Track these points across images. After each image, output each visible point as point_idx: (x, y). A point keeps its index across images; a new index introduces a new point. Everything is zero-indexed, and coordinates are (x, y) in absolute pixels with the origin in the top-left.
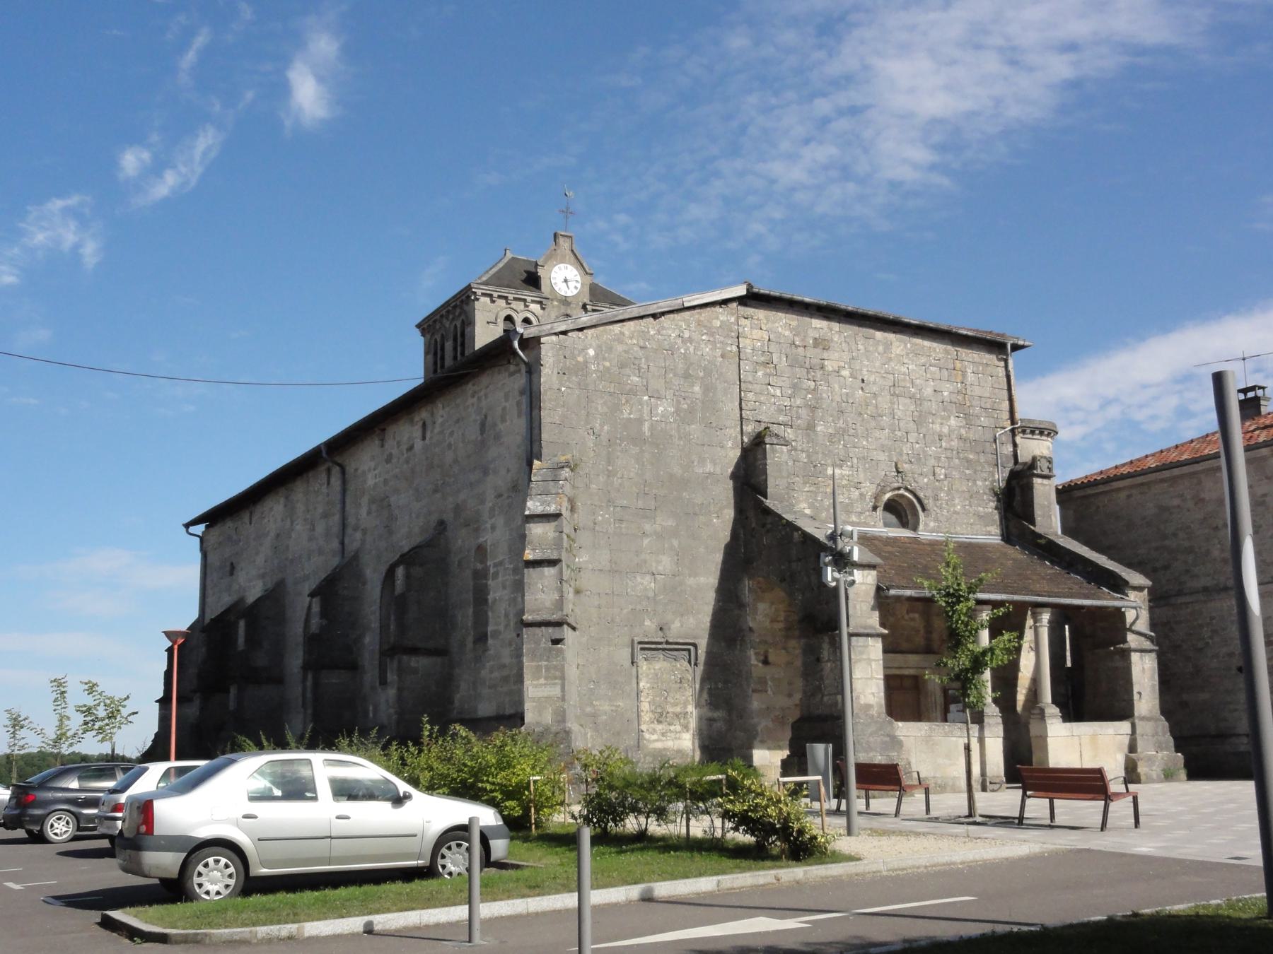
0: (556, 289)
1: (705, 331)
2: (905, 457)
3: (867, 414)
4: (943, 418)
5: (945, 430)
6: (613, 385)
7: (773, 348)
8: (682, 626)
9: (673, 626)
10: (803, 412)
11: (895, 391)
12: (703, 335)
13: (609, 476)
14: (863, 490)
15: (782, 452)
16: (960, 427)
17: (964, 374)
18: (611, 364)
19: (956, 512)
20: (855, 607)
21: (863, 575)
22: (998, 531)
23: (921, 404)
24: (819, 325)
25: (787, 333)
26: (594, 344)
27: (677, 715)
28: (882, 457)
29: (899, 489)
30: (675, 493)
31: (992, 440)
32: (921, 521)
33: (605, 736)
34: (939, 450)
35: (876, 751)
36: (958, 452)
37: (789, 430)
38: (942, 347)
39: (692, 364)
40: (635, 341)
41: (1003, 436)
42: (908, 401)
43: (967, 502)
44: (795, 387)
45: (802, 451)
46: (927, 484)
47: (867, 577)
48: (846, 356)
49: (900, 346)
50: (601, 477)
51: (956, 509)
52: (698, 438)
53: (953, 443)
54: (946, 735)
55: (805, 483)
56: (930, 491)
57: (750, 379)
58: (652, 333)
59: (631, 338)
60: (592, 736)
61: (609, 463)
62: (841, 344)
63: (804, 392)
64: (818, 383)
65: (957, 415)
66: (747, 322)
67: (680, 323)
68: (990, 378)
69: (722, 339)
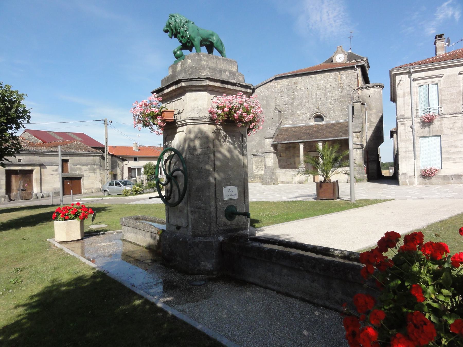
4: (333, 92)
5: (334, 95)
19: (336, 115)
24: (296, 79)
27: (261, 168)
28: (313, 106)
29: (317, 113)
34: (331, 100)
42: (321, 90)
43: (340, 112)
44: (288, 95)
54: (290, 172)
55: (290, 117)
57: (277, 96)
66: (276, 84)
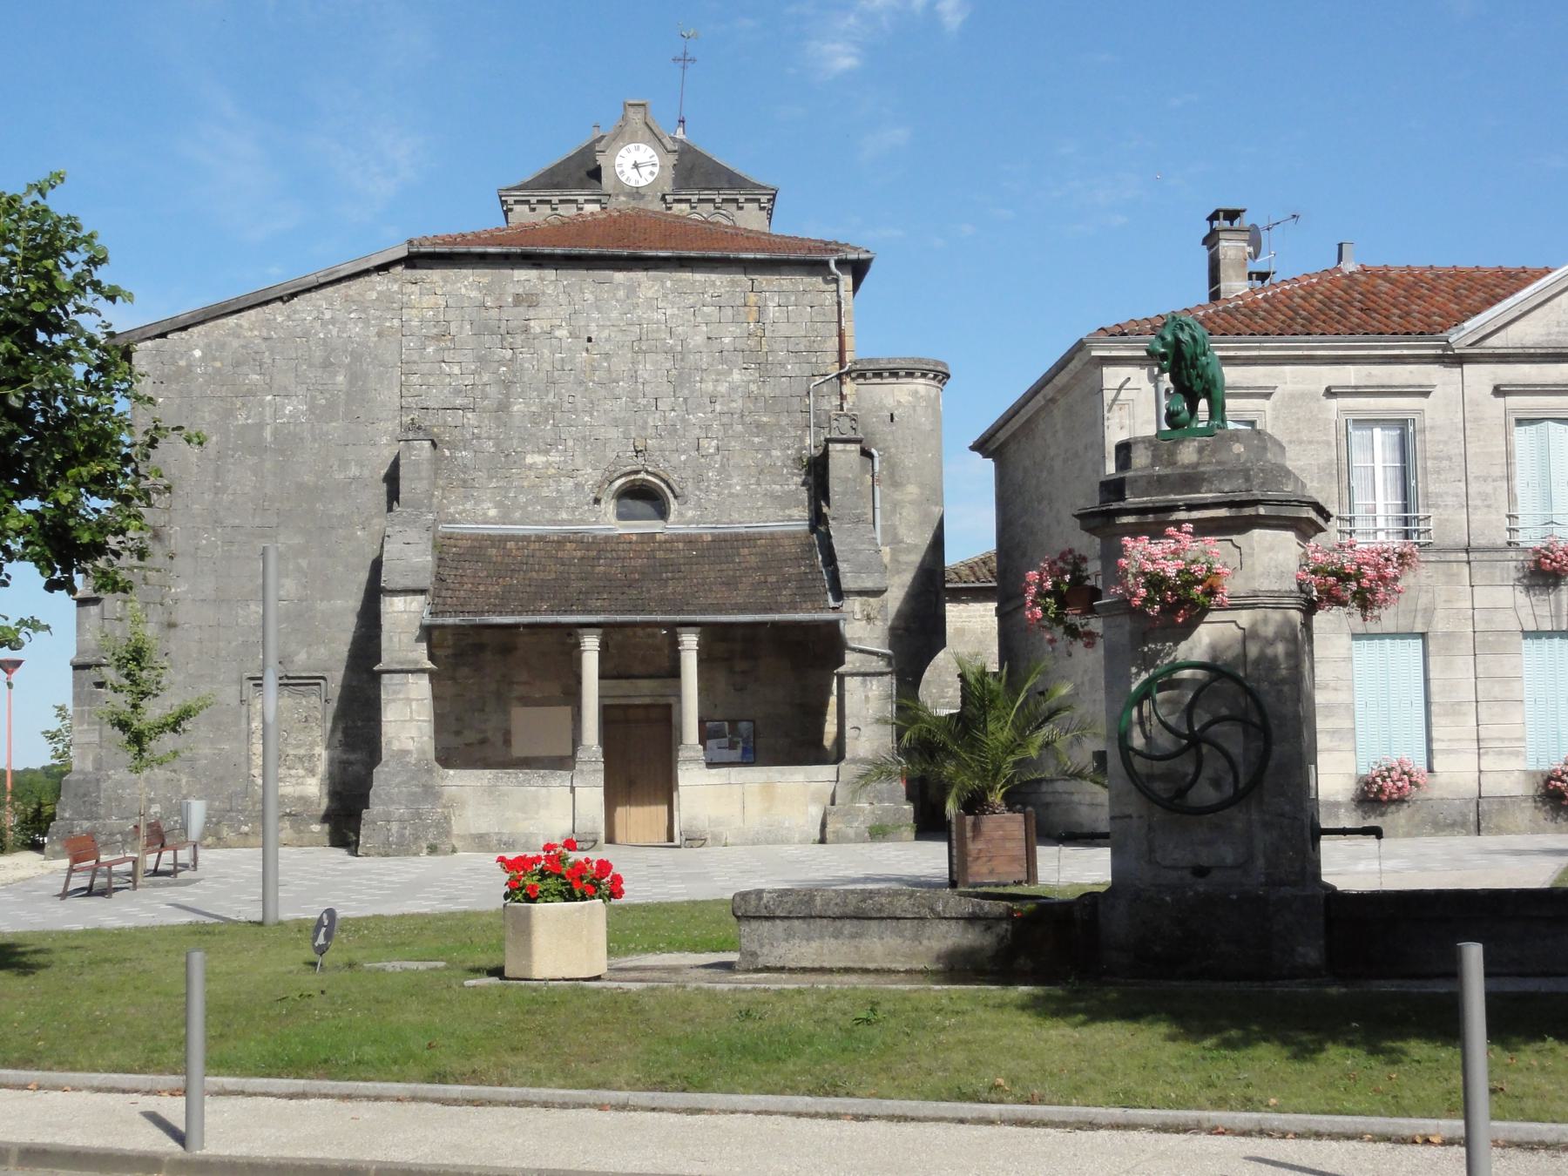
0: (623, 179)
1: (354, 308)
2: (651, 431)
3: (593, 381)
4: (719, 373)
5: (723, 388)
6: (225, 388)
7: (451, 315)
8: (309, 658)
9: (296, 659)
10: (492, 391)
11: (641, 347)
12: (351, 313)
13: (216, 494)
14: (580, 479)
15: (422, 448)
16: (749, 382)
17: (761, 309)
18: (222, 363)
19: (731, 495)
20: (391, 638)
21: (405, 601)
22: (806, 515)
23: (682, 360)
24: (524, 277)
25: (473, 294)
26: (201, 344)
27: (300, 759)
28: (614, 433)
29: (637, 472)
30: (304, 505)
31: (805, 393)
32: (672, 510)
33: (204, 781)
34: (710, 415)
35: (400, 804)
36: (742, 416)
37: (469, 415)
38: (727, 278)
39: (333, 350)
40: (256, 333)
41: (824, 386)
42: (661, 357)
43: (753, 481)
44: (481, 360)
45: (489, 438)
46: (685, 463)
47: (411, 603)
48: (565, 311)
49: (653, 286)
50: (206, 496)
51: (733, 491)
52: (339, 437)
53: (734, 405)
54: (520, 784)
55: (490, 478)
56: (689, 472)
57: (416, 357)
58: (280, 319)
59: (251, 330)
60: (187, 782)
61: (217, 478)
62: (557, 296)
63: (496, 365)
64: (518, 351)
65: (745, 366)
66: (415, 288)
67: (320, 303)
68: (809, 309)
69: (378, 313)
